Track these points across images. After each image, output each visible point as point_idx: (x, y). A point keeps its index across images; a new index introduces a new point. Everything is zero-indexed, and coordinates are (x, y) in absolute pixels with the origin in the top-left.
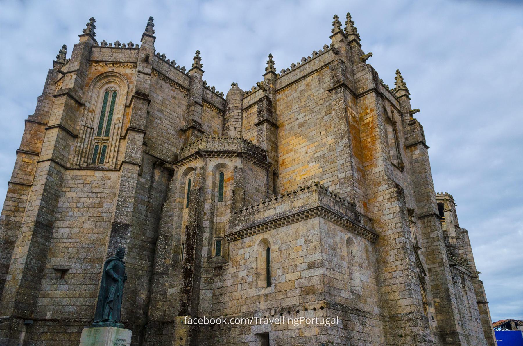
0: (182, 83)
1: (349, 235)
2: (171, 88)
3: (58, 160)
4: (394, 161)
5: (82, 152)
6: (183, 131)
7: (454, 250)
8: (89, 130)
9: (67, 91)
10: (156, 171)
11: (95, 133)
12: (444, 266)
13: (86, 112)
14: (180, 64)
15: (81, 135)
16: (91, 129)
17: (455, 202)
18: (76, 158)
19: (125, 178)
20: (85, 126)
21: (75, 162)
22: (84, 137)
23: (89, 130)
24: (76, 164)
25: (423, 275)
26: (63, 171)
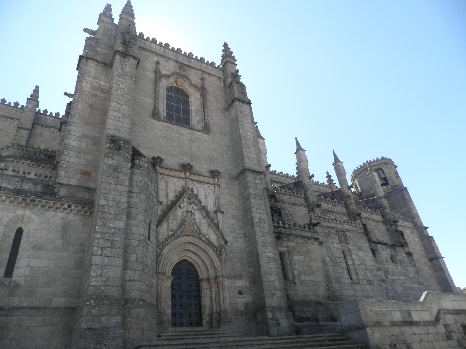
1: (20, 212)
4: (199, 125)
7: (384, 209)
12: (253, 226)
17: (395, 164)
25: (222, 242)
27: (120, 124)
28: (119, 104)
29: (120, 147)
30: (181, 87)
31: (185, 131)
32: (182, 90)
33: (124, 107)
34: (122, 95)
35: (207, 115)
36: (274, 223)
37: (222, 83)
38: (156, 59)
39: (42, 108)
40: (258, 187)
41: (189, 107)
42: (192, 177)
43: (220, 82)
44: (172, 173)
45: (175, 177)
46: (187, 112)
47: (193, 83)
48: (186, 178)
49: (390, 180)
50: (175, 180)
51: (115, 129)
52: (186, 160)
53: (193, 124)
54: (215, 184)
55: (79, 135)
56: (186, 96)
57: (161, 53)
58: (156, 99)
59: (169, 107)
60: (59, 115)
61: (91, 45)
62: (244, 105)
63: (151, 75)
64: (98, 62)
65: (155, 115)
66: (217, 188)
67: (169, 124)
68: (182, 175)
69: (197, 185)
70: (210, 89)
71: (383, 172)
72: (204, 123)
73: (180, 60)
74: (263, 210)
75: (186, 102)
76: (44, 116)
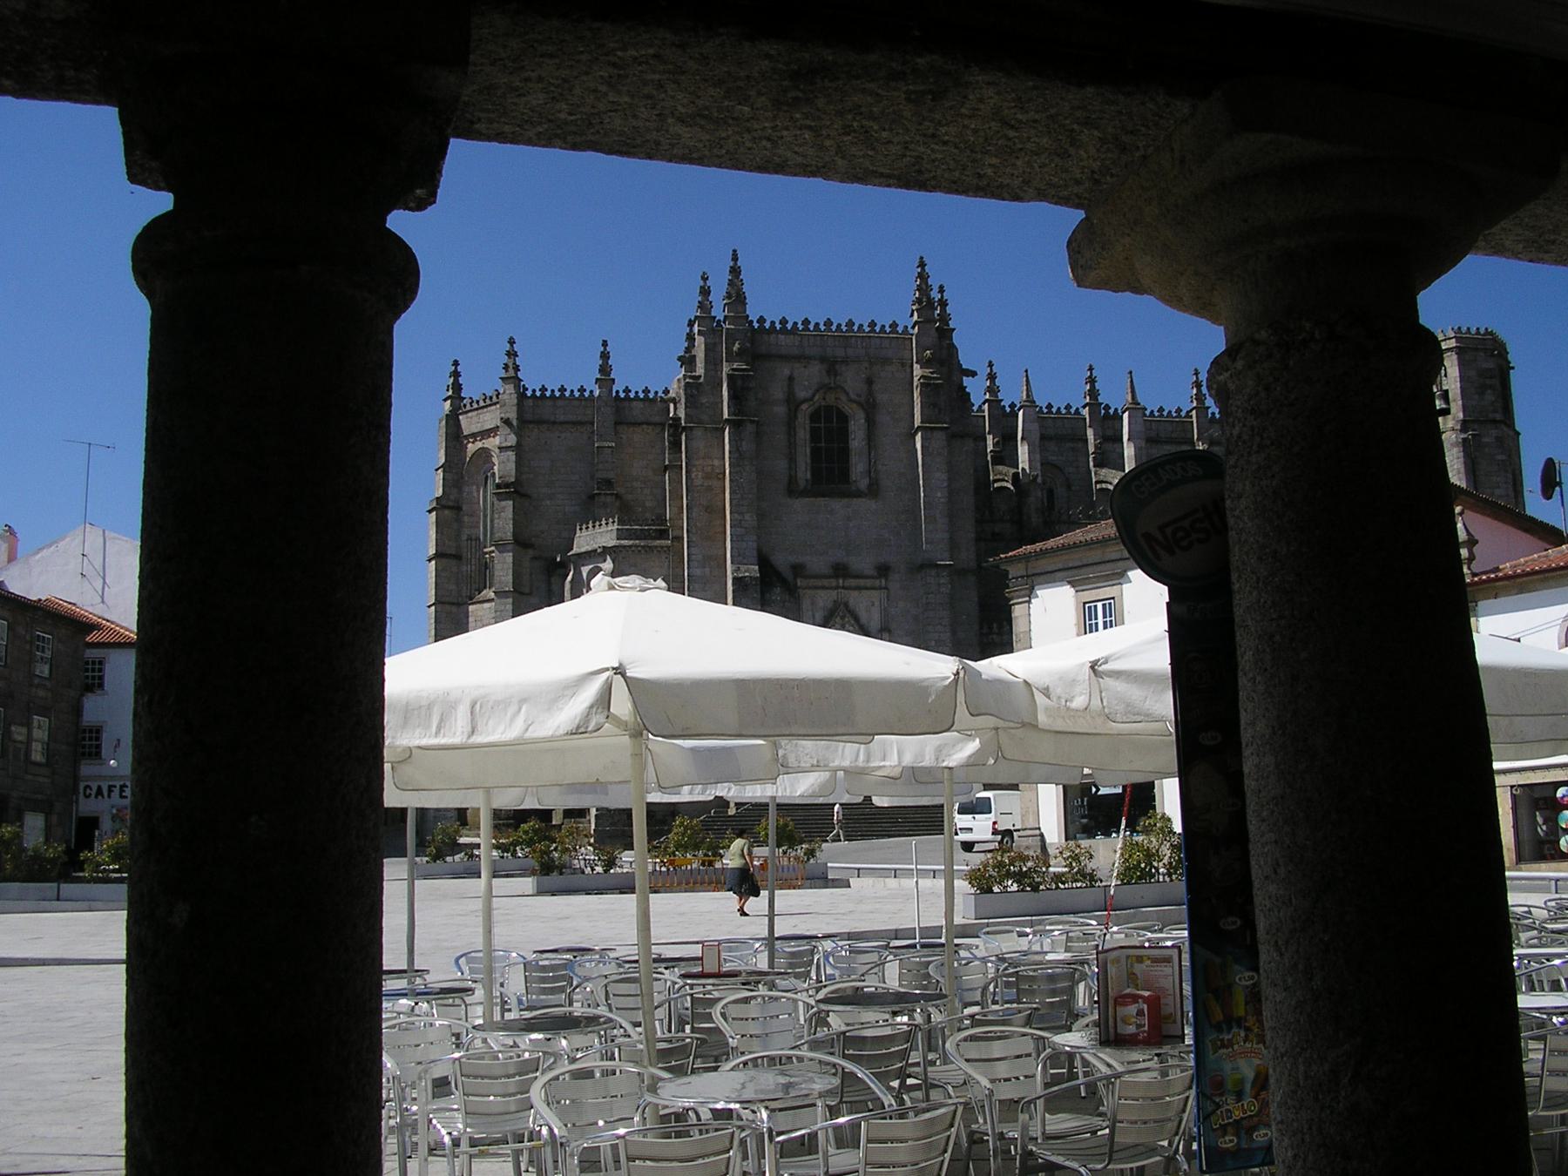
2: (563, 435)
5: (471, 577)
8: (474, 543)
9: (434, 505)
10: (553, 579)
13: (466, 519)
14: (572, 386)
15: (464, 554)
16: (476, 540)
18: (465, 588)
19: (498, 613)
20: (467, 540)
21: (464, 595)
22: (469, 556)
23: (474, 543)
24: (467, 596)
26: (454, 609)
27: (744, 544)
28: (739, 514)
30: (835, 404)
31: (837, 504)
32: (838, 408)
33: (747, 517)
35: (875, 462)
36: (981, 628)
37: (909, 370)
38: (787, 372)
39: (618, 387)
40: (943, 589)
41: (848, 443)
42: (847, 584)
44: (819, 583)
45: (823, 588)
46: (845, 452)
47: (853, 396)
48: (837, 588)
49: (1454, 400)
50: (822, 593)
53: (854, 479)
54: (881, 588)
55: (700, 557)
56: (844, 419)
59: (815, 453)
60: (649, 392)
63: (780, 410)
65: (792, 490)
66: (883, 594)
68: (833, 582)
69: (856, 593)
70: (882, 398)
71: (1446, 376)
72: (868, 479)
74: (945, 626)
75: (843, 434)
76: (626, 404)
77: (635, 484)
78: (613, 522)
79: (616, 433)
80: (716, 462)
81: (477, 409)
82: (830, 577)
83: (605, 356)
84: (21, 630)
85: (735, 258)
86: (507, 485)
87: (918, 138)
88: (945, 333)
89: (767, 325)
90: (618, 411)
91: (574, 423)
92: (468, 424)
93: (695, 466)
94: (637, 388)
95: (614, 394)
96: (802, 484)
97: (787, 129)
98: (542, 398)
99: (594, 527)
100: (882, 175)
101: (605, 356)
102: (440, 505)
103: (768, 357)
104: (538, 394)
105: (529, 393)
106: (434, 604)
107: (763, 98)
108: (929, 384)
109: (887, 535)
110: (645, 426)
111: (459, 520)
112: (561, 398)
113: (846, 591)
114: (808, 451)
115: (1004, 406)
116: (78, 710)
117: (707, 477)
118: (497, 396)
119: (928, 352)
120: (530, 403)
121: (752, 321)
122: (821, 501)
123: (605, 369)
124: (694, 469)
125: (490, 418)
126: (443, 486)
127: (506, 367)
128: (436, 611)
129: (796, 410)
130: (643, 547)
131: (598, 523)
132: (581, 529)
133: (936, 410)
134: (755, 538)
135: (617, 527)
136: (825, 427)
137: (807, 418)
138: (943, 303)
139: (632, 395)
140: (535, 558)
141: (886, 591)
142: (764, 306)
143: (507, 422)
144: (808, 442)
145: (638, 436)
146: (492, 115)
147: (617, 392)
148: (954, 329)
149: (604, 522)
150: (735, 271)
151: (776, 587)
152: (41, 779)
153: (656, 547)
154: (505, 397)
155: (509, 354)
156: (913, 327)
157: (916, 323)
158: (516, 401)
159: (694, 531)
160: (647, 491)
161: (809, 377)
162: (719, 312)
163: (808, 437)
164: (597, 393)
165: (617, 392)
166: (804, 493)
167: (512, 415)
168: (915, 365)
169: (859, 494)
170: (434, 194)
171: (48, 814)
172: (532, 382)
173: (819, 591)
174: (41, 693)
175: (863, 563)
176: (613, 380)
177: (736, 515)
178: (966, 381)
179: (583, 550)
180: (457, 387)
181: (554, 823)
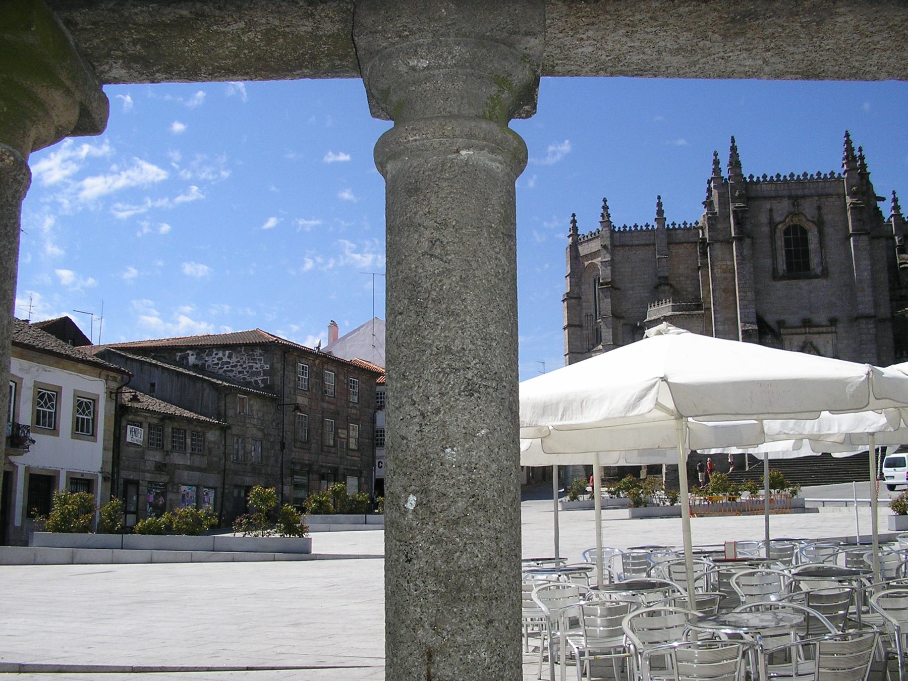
0: (647, 242)
3: (574, 350)
6: (656, 287)
11: (594, 318)
13: (584, 304)
14: (641, 224)
15: (584, 325)
20: (585, 316)
29: (750, 335)
31: (803, 284)
32: (800, 225)
33: (749, 294)
34: (746, 283)
36: (896, 353)
37: (843, 199)
38: (768, 206)
39: (668, 222)
40: (871, 331)
43: (840, 200)
44: (794, 331)
45: (797, 334)
46: (806, 253)
47: (809, 218)
48: (806, 333)
51: (745, 317)
52: (806, 314)
54: (832, 332)
55: (722, 319)
56: (804, 232)
57: (773, 194)
58: (774, 258)
59: (788, 254)
61: (712, 224)
62: (862, 237)
63: (766, 229)
64: (721, 242)
65: (775, 277)
67: (788, 281)
68: (803, 330)
69: (817, 336)
70: (828, 218)
73: (793, 192)
75: (805, 241)
77: (681, 278)
78: (670, 301)
79: (669, 249)
80: (729, 263)
81: (587, 241)
82: (801, 327)
83: (659, 205)
84: (342, 377)
85: (733, 141)
86: (607, 284)
87: (810, 48)
88: (864, 175)
89: (755, 179)
90: (669, 236)
91: (643, 245)
92: (583, 250)
93: (716, 266)
94: (679, 222)
95: (666, 227)
96: (781, 272)
97: (732, 51)
98: (624, 232)
99: (658, 304)
100: (791, 73)
101: (659, 205)
102: (569, 297)
103: (757, 198)
104: (622, 229)
105: (617, 230)
106: (567, 354)
107: (717, 35)
108: (856, 207)
109: (834, 300)
110: (685, 244)
111: (580, 305)
112: (636, 231)
113: (811, 336)
114: (784, 253)
115: (904, 218)
116: (373, 421)
117: (724, 272)
118: (598, 232)
119: (854, 188)
120: (618, 235)
121: (745, 178)
122: (793, 282)
123: (660, 212)
124: (715, 268)
125: (595, 246)
126: (570, 286)
127: (603, 215)
128: (569, 358)
129: (775, 230)
130: (688, 315)
131: (660, 303)
132: (651, 306)
133: (861, 223)
134: (754, 306)
135: (671, 304)
136: (793, 238)
137: (782, 233)
138: (862, 158)
139: (677, 226)
140: (625, 324)
141: (835, 334)
142: (751, 169)
143: (604, 247)
144: (783, 247)
145: (681, 251)
146: (564, 62)
147: (668, 225)
148: (870, 173)
149: (664, 301)
150: (734, 149)
151: (768, 335)
152: (355, 458)
153: (696, 314)
154: (603, 233)
155: (603, 207)
156: (844, 174)
157: (846, 171)
158: (609, 235)
159: (717, 304)
160: (689, 282)
161: (782, 208)
162: (725, 174)
163: (783, 244)
164: (656, 227)
165: (668, 225)
166: (783, 278)
167: (608, 242)
168: (847, 197)
169: (816, 277)
170: (535, 108)
171: (359, 478)
172: (618, 222)
173: (794, 336)
174: (354, 411)
175: (821, 318)
176: (665, 218)
177: (742, 294)
178: (879, 204)
179: (652, 318)
180: (575, 229)
181: (641, 478)
